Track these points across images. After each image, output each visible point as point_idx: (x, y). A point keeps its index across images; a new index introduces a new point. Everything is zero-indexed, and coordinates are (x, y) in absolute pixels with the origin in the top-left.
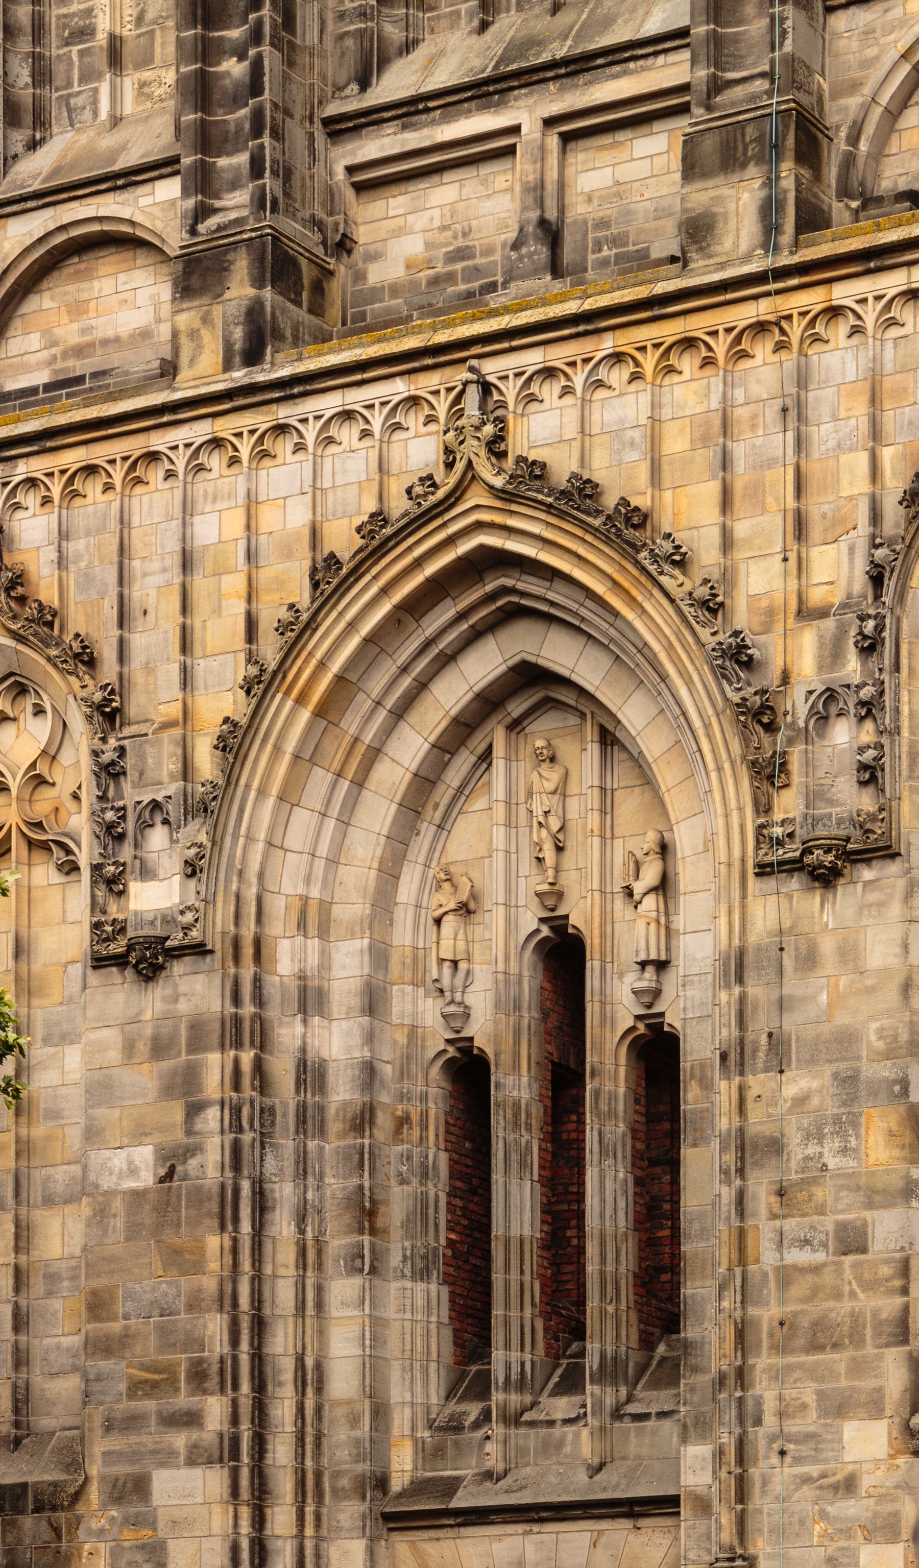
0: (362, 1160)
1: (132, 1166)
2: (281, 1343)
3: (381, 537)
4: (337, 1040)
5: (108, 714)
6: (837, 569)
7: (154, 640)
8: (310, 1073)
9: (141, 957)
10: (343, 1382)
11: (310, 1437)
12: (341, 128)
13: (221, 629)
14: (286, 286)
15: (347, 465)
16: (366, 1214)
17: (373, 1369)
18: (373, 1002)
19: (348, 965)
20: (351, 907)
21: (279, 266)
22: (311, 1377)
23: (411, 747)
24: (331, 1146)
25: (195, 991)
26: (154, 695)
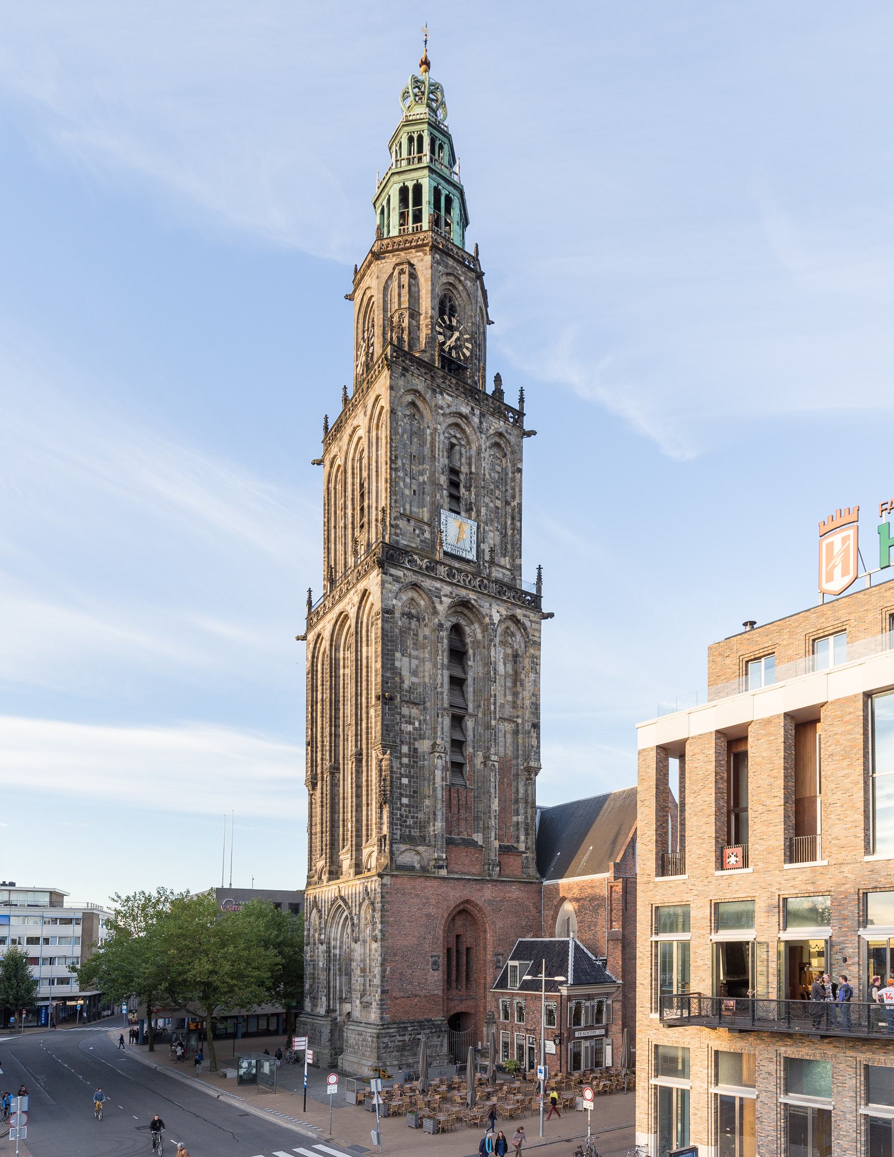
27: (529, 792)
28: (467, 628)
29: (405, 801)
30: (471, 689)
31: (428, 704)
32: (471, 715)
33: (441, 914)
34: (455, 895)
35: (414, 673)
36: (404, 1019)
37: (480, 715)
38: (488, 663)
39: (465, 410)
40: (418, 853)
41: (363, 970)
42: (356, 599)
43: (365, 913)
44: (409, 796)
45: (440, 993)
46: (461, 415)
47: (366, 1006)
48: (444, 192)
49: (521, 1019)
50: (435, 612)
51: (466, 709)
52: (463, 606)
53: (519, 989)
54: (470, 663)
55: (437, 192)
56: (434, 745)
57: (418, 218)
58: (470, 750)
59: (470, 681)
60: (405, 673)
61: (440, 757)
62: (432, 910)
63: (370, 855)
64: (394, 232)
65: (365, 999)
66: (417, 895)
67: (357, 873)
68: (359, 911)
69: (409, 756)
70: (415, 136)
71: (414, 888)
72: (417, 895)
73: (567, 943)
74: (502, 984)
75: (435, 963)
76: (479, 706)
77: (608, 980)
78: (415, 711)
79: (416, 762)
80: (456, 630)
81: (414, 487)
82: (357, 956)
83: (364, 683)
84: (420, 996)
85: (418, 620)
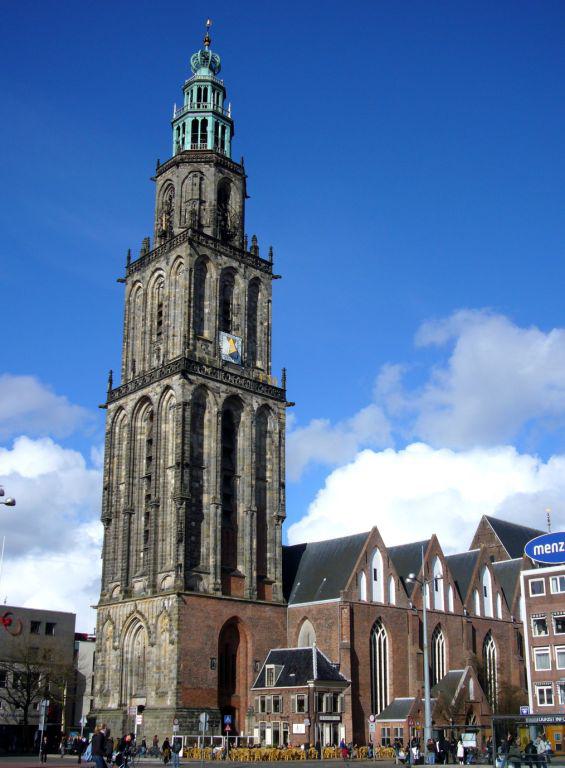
0: (131, 666)
1: (114, 666)
3: (130, 614)
5: (114, 628)
8: (127, 659)
9: (115, 649)
14: (128, 593)
15: (128, 607)
16: (131, 671)
17: (131, 684)
18: (132, 653)
20: (131, 643)
21: (126, 592)
22: (126, 685)
27: (278, 535)
28: (234, 413)
33: (218, 626)
34: (228, 611)
36: (192, 706)
39: (235, 264)
41: (159, 668)
42: (159, 390)
43: (164, 623)
45: (216, 688)
46: (232, 268)
47: (162, 695)
49: (276, 710)
53: (277, 685)
55: (216, 125)
57: (204, 138)
62: (211, 623)
63: (165, 579)
64: (188, 147)
65: (160, 690)
66: (202, 610)
67: (154, 592)
70: (203, 88)
71: (200, 605)
72: (202, 610)
73: (311, 650)
74: (261, 683)
75: (213, 665)
77: (341, 680)
82: (153, 657)
83: (162, 450)
84: (202, 689)
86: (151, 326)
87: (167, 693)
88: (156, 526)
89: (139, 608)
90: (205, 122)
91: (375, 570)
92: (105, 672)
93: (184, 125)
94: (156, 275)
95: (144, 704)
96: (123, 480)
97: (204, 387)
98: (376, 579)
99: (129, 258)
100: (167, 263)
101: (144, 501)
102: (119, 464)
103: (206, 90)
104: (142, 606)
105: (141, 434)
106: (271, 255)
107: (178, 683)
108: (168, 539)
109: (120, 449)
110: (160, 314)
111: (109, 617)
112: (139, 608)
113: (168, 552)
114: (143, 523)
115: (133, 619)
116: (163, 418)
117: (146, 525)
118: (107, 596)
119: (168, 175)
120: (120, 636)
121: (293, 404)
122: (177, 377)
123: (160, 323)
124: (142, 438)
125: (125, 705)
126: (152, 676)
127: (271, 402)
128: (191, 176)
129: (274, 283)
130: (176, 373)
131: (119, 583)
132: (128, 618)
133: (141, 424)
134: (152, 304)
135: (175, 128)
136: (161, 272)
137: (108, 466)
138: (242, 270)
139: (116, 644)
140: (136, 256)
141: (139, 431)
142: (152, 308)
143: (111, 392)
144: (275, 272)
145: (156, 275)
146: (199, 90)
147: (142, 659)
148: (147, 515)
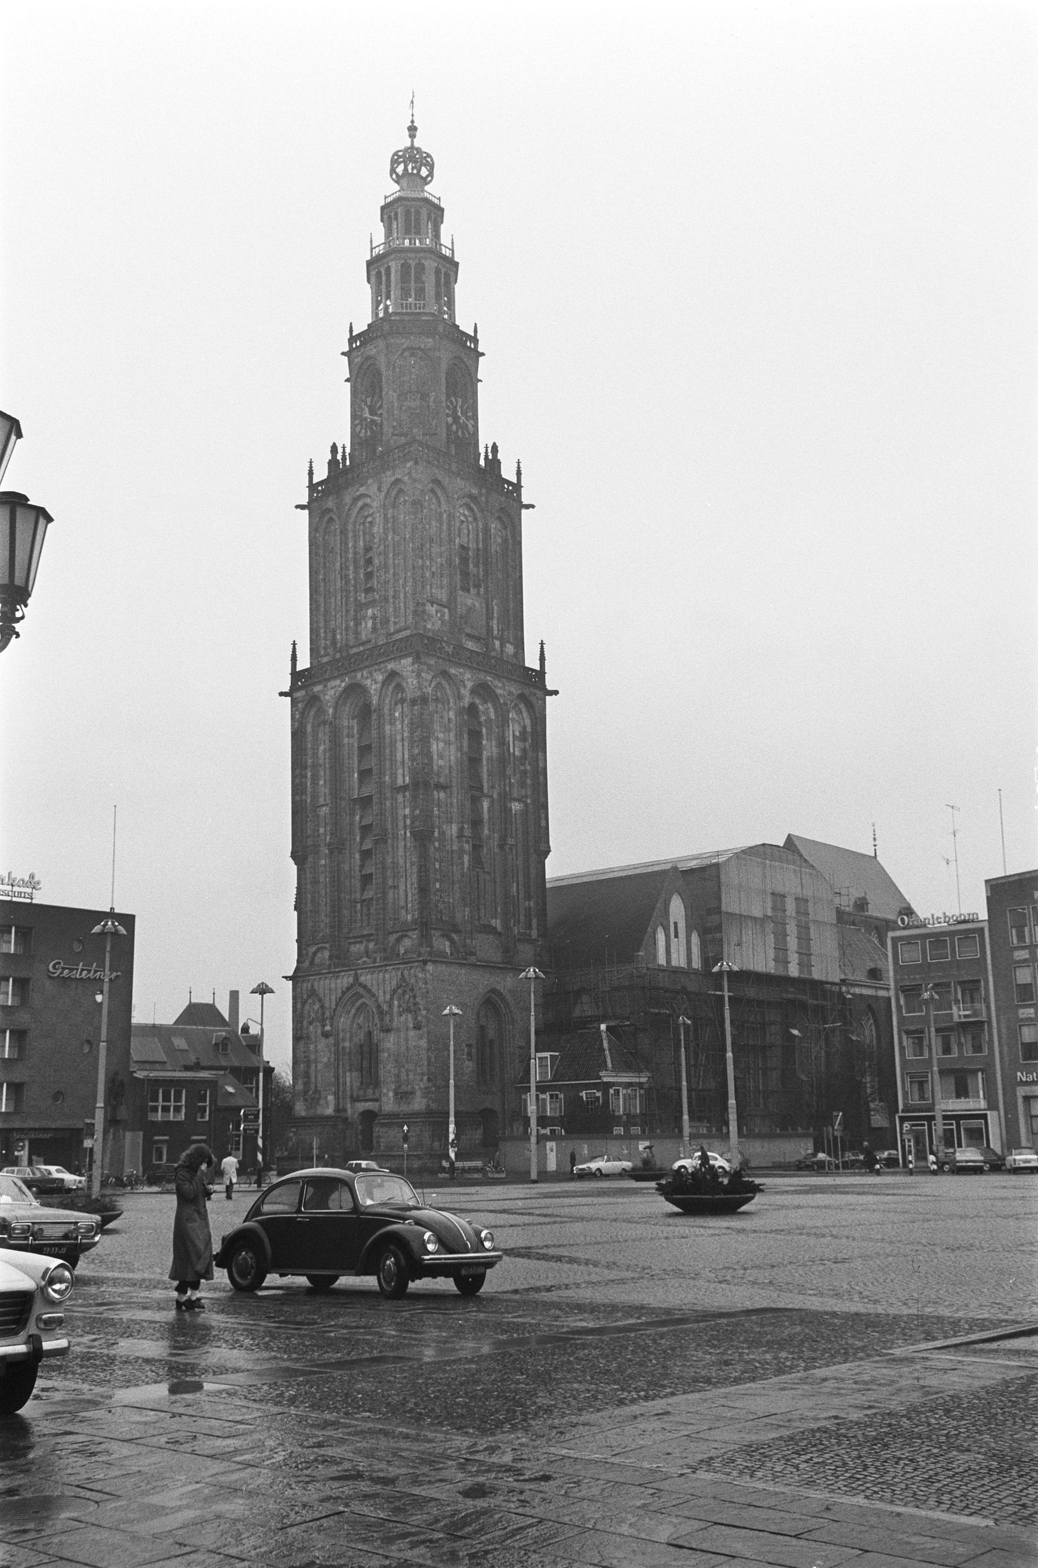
1: (325, 1060)
2: (341, 1080)
3: (348, 989)
4: (347, 1044)
6: (388, 997)
7: (327, 999)
8: (344, 1048)
9: (326, 1035)
10: (348, 1084)
11: (344, 1091)
12: (347, 938)
13: (333, 998)
15: (346, 980)
17: (351, 1082)
18: (351, 1040)
19: (348, 1036)
22: (345, 1084)
23: (353, 1011)
24: (346, 1057)
25: (331, 1040)
26: (327, 1005)
29: (438, 885)
30: (485, 769)
31: (455, 789)
32: (487, 796)
35: (441, 756)
37: (495, 796)
38: (502, 742)
39: (475, 491)
40: (451, 940)
42: (380, 678)
44: (441, 882)
48: (443, 270)
50: (459, 697)
51: (481, 789)
52: (483, 690)
54: (484, 742)
55: (438, 272)
56: (461, 830)
58: (486, 832)
59: (484, 762)
60: (435, 757)
61: (467, 842)
68: (392, 999)
69: (439, 840)
70: (413, 210)
75: (469, 1054)
76: (493, 787)
78: (442, 795)
79: (444, 846)
80: (472, 709)
81: (433, 569)
83: (388, 763)
85: (443, 704)
86: (355, 579)
87: (413, 1093)
88: (384, 868)
89: (362, 979)
90: (421, 268)
91: (676, 924)
92: (308, 1067)
93: (388, 270)
94: (360, 504)
95: (376, 1110)
96: (321, 801)
97: (445, 674)
98: (676, 936)
99: (311, 473)
100: (379, 489)
101: (357, 831)
102: (315, 778)
103: (418, 213)
104: (366, 978)
105: (348, 736)
106: (519, 473)
107: (429, 1080)
108: (402, 888)
109: (315, 755)
110: (369, 562)
111: (313, 993)
112: (362, 979)
113: (402, 903)
114: (358, 862)
115: (355, 993)
116: (387, 717)
117: (362, 866)
118: (307, 963)
119: (371, 350)
120: (332, 1018)
121: (556, 693)
122: (410, 660)
123: (369, 576)
124: (351, 743)
125: (345, 1110)
126: (387, 1069)
127: (527, 692)
128: (406, 354)
129: (524, 511)
130: (405, 656)
131: (327, 945)
132: (343, 993)
133: (349, 723)
134: (355, 547)
135: (373, 273)
136: (368, 500)
137: (297, 781)
138: (483, 499)
139: (328, 1028)
140: (321, 474)
141: (345, 732)
142: (355, 553)
143: (296, 675)
144: (525, 500)
145: (360, 504)
146: (407, 213)
147: (366, 1049)
148: (366, 855)
